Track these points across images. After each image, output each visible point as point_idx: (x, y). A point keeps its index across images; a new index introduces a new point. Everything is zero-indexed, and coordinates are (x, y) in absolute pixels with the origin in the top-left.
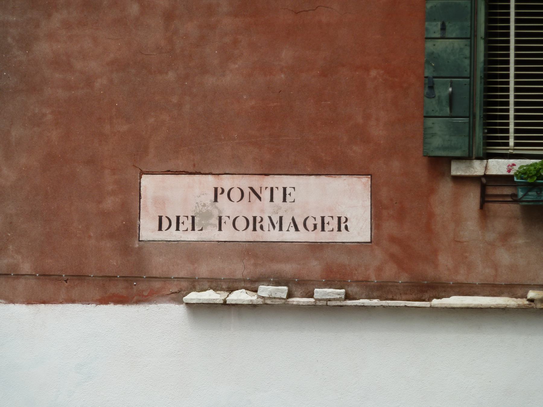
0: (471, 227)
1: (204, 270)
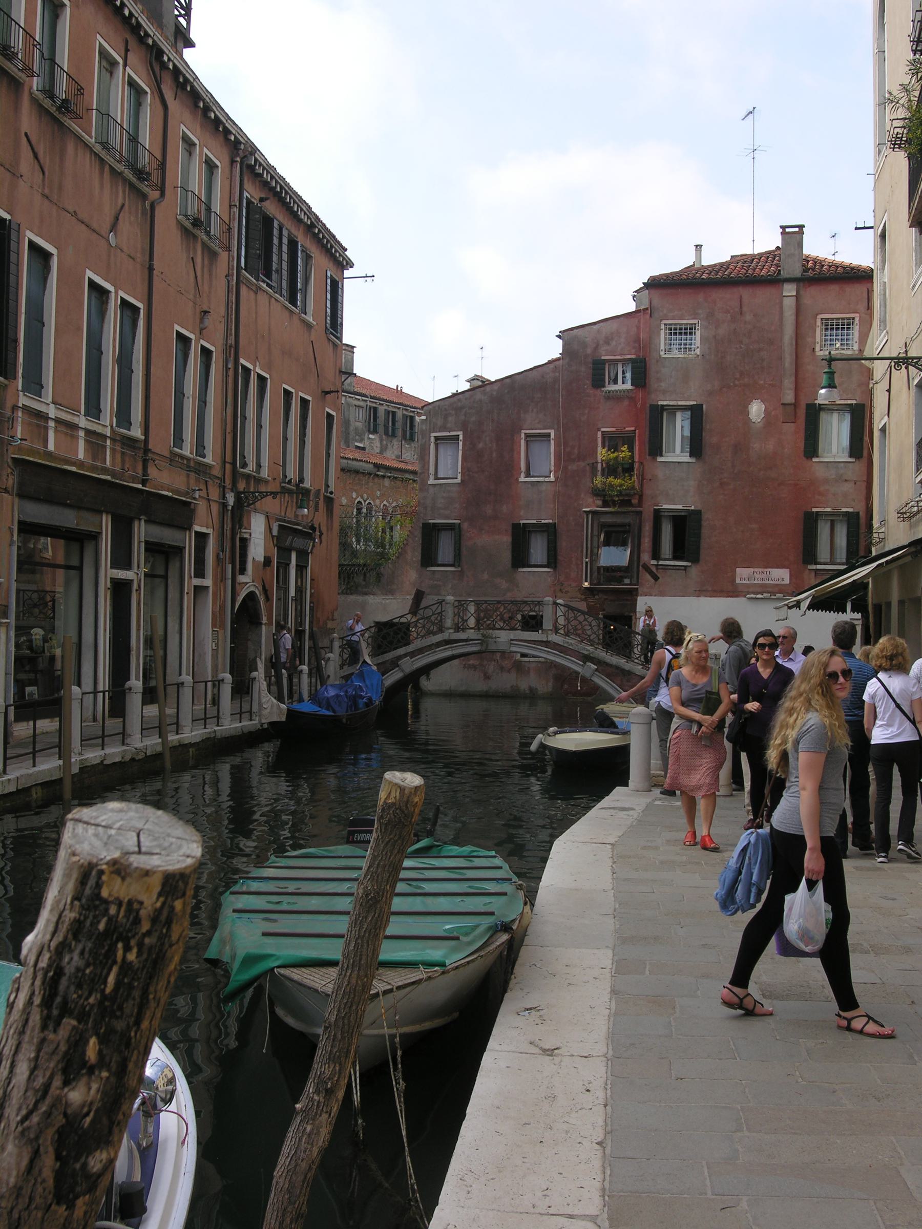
1: (751, 590)
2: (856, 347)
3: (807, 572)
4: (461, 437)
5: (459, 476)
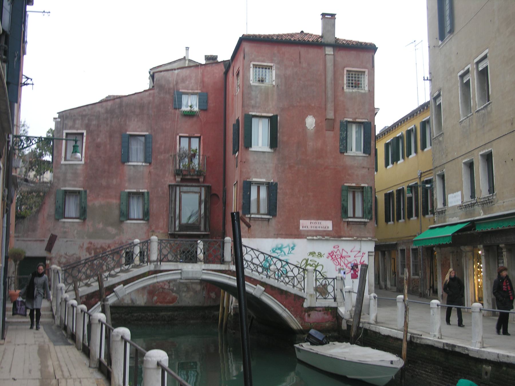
1: (309, 234)
2: (367, 88)
3: (342, 223)
4: (85, 134)
5: (83, 159)
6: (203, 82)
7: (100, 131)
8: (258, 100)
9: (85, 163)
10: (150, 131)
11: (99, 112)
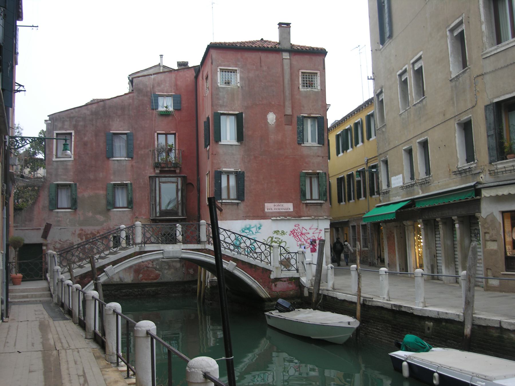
0: (305, 209)
1: (273, 215)
2: (319, 88)
3: (302, 204)
4: (73, 134)
5: (72, 156)
6: (176, 85)
7: (87, 131)
8: (225, 100)
9: (74, 159)
10: (131, 130)
11: (85, 113)
